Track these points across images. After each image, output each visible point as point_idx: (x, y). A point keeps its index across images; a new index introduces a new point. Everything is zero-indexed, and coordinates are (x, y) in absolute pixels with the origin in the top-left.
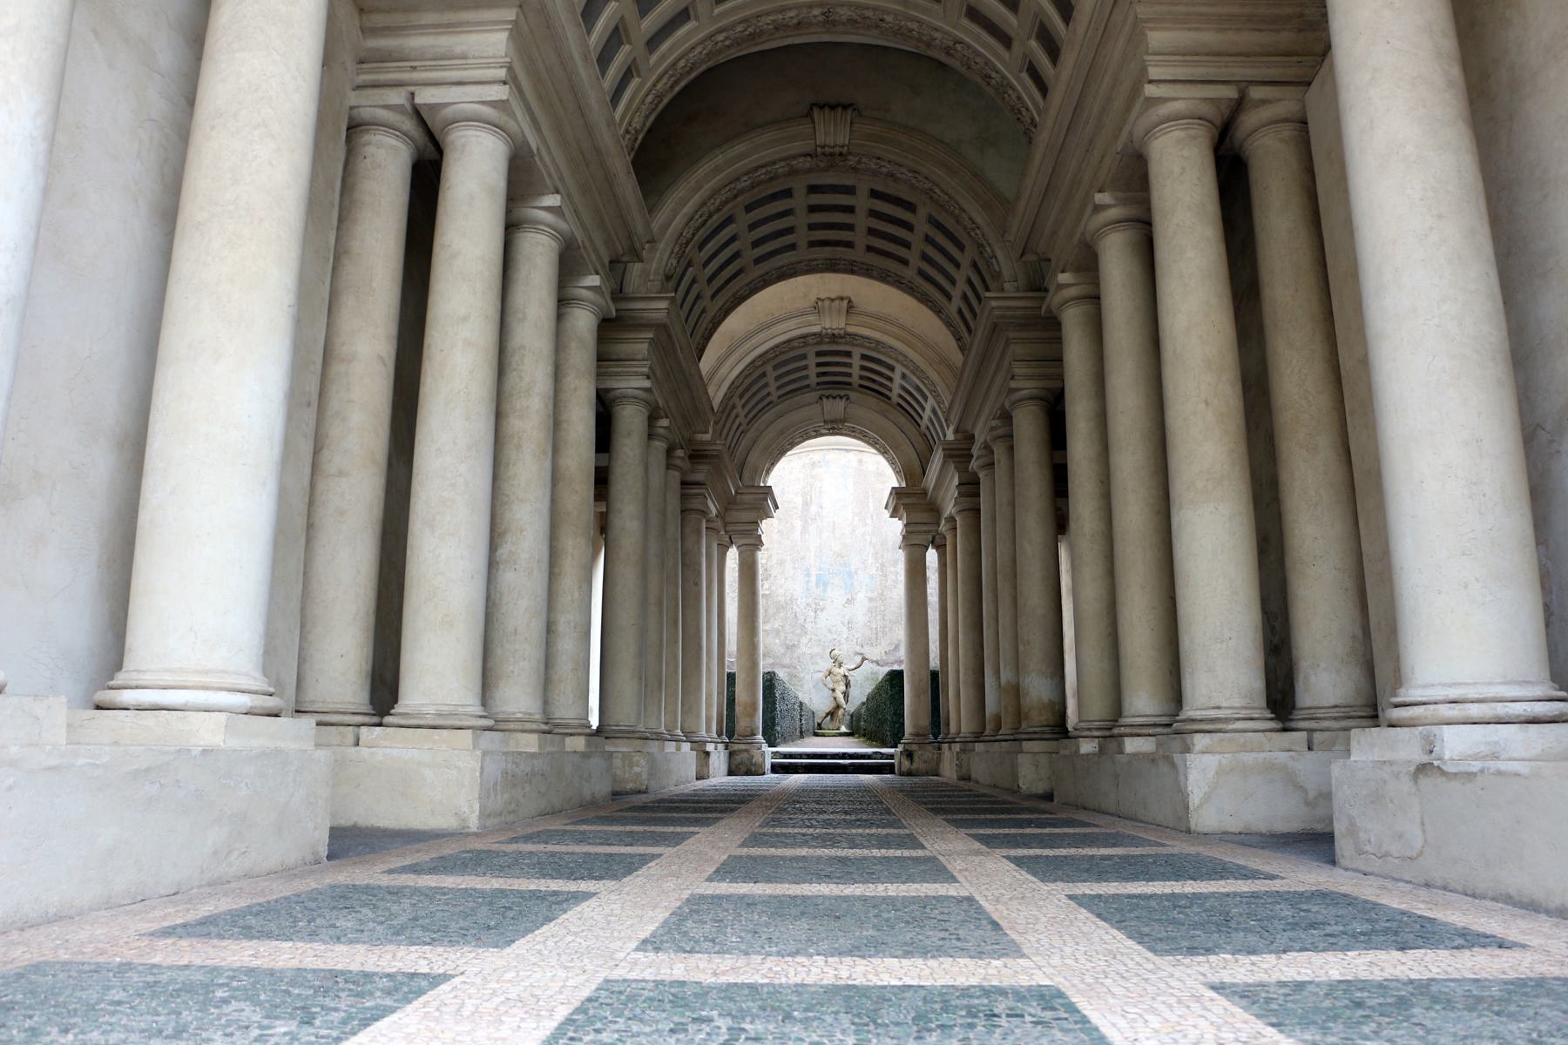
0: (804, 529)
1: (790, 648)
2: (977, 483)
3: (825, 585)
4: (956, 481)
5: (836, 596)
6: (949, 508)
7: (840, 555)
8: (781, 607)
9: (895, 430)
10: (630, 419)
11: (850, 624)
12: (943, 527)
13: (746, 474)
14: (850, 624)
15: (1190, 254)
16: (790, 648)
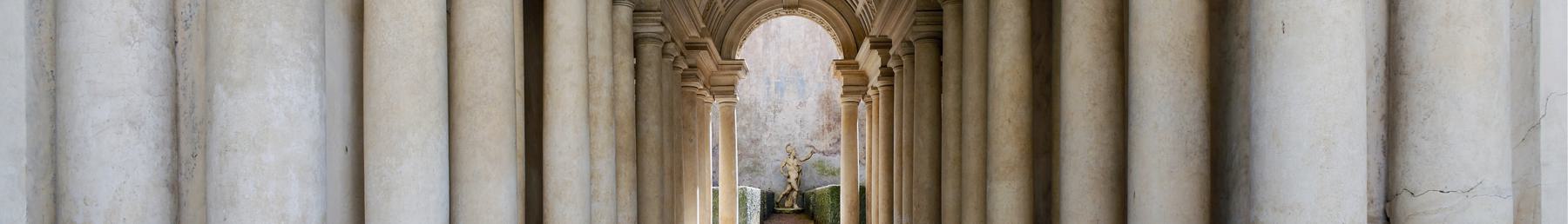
0: (766, 45)
1: (755, 142)
2: (892, 74)
3: (782, 90)
4: (879, 63)
5: (791, 99)
6: (874, 81)
7: (794, 66)
8: (746, 109)
9: (836, 14)
10: (650, 51)
11: (802, 123)
12: (870, 92)
13: (725, 48)
14: (802, 123)
15: (1007, 26)
16: (755, 142)
